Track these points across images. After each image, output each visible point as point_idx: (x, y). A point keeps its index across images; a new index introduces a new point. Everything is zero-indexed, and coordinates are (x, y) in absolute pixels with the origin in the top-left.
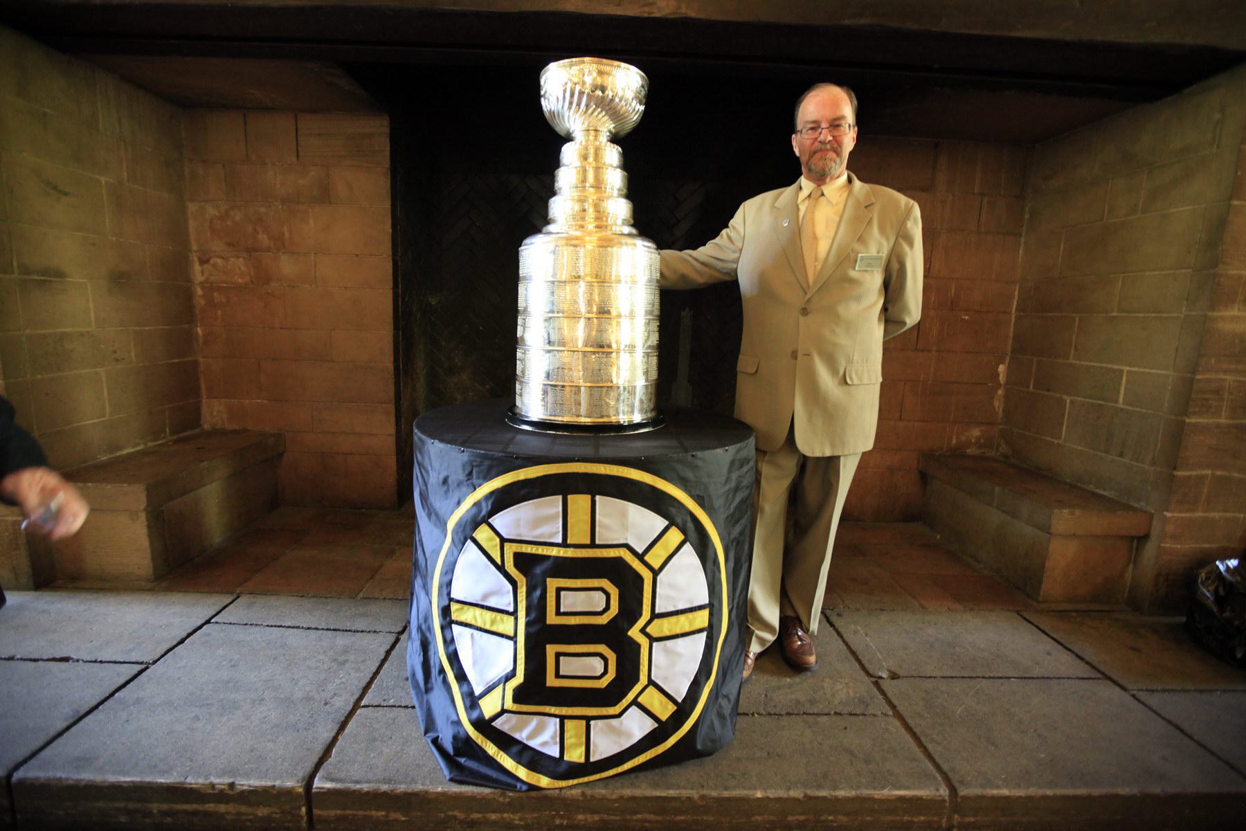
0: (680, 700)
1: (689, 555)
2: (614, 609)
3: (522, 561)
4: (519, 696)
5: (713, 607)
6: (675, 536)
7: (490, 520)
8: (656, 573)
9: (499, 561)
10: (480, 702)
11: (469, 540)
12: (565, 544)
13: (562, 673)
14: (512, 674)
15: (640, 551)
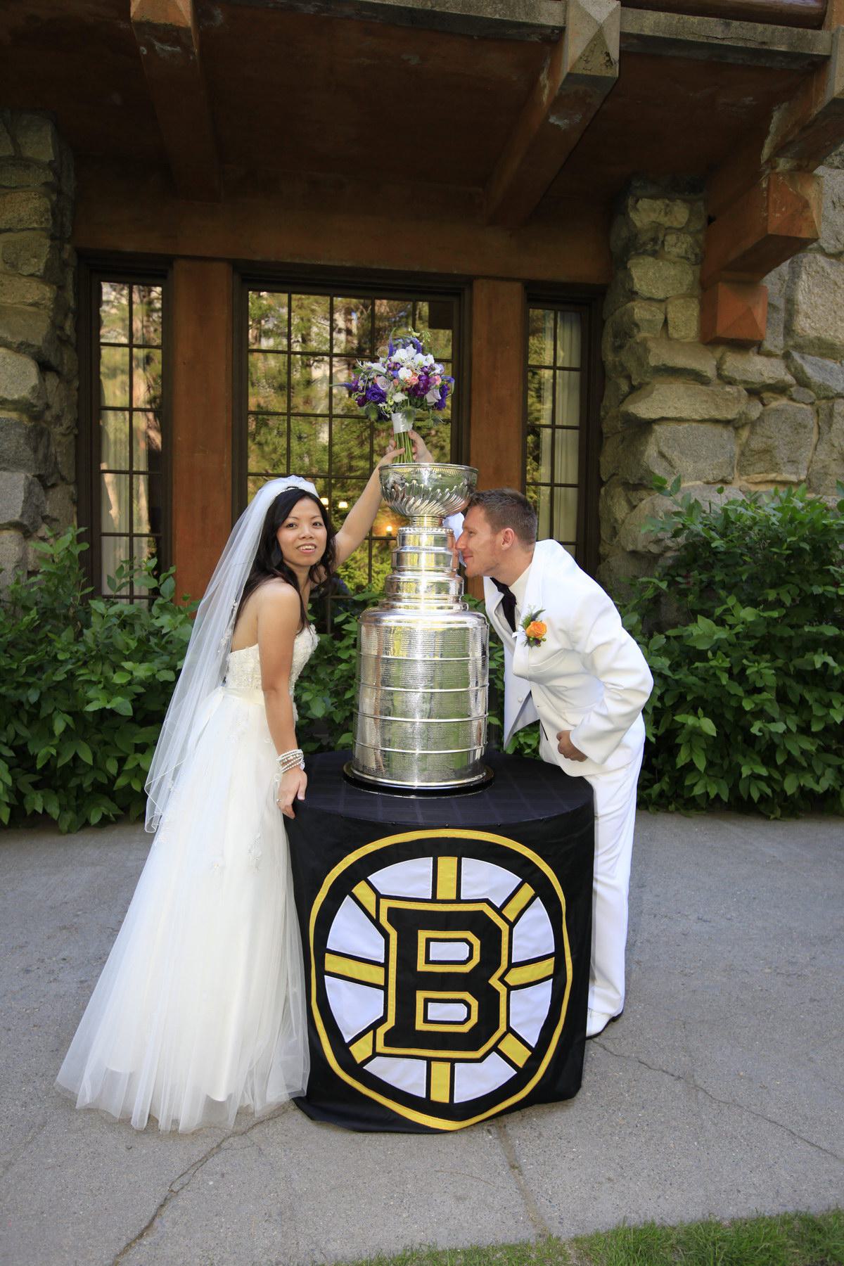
0: (533, 1046)
1: (539, 909)
2: (477, 958)
3: (394, 915)
4: (390, 1039)
5: (558, 954)
6: (528, 891)
7: (369, 878)
8: (512, 925)
9: (374, 915)
10: (351, 1048)
11: (348, 896)
12: (434, 900)
13: (429, 1018)
14: (383, 1020)
15: (498, 906)
